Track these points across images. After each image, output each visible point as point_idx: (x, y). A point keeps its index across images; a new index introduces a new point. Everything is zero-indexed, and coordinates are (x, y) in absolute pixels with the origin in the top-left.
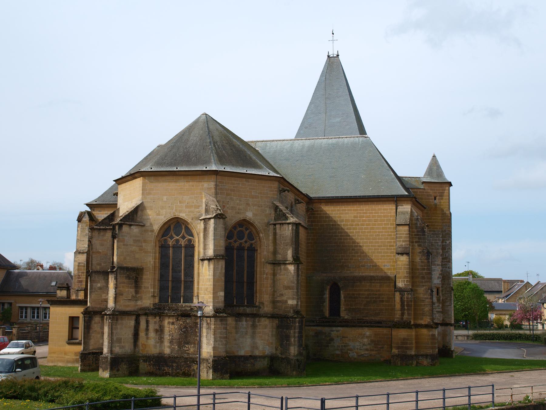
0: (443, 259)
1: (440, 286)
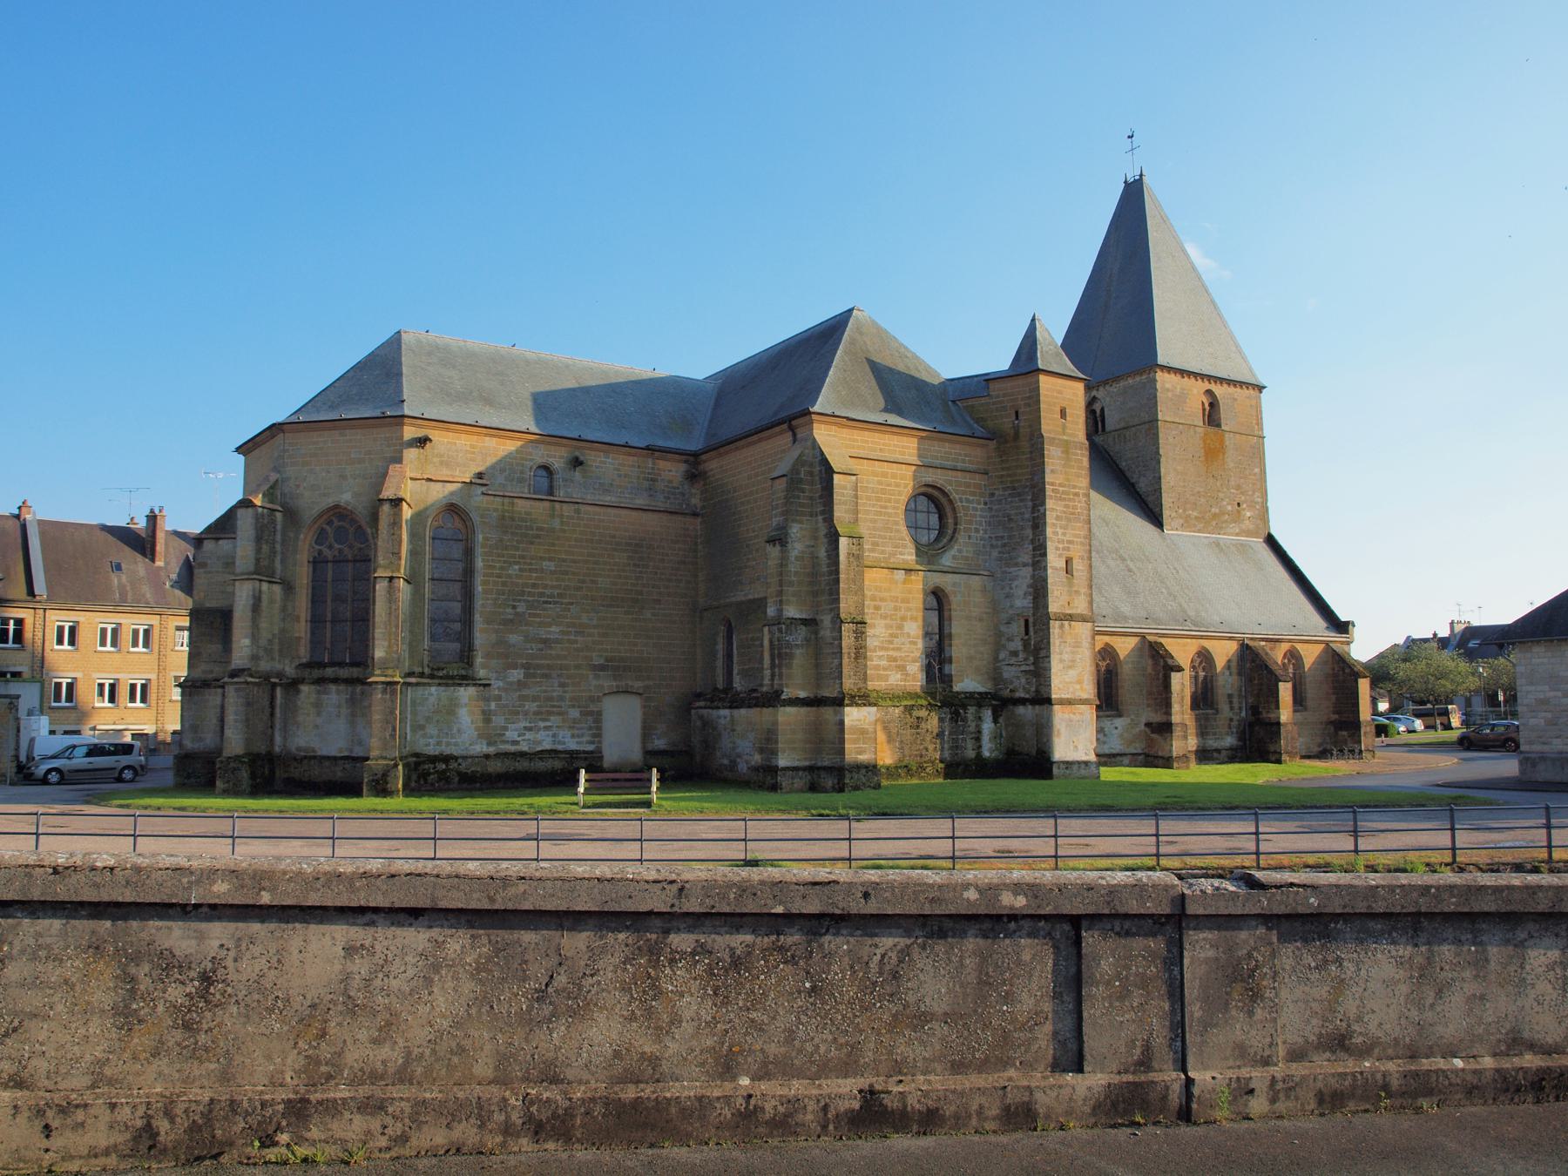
0: (1034, 549)
1: (1030, 613)
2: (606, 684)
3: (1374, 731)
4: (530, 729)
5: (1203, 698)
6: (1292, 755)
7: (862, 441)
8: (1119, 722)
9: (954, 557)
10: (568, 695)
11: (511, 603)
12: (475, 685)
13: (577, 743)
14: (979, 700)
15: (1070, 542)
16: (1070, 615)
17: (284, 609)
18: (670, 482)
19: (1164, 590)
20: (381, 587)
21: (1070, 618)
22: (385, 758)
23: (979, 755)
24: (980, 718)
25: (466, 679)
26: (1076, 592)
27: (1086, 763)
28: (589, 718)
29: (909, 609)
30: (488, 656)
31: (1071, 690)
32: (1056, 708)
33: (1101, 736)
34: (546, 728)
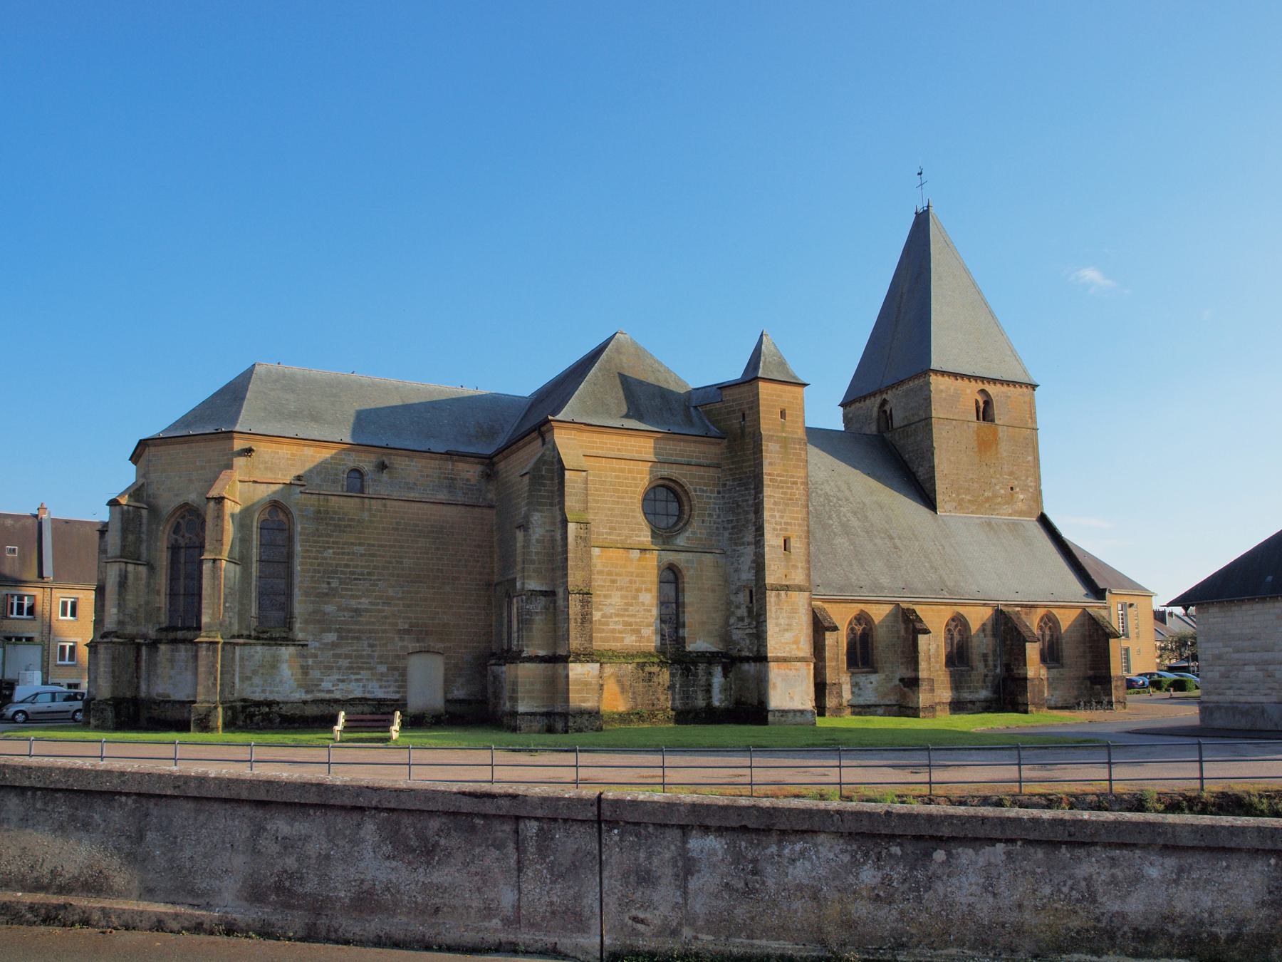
2: (410, 646)
3: (1125, 685)
4: (343, 681)
5: (958, 657)
6: (1039, 706)
7: (601, 443)
8: (873, 678)
9: (688, 538)
10: (376, 654)
11: (325, 580)
12: (294, 645)
13: (385, 692)
14: (709, 658)
15: (786, 523)
16: (787, 586)
17: (148, 585)
18: (468, 480)
19: (926, 564)
20: (207, 567)
21: (787, 588)
22: (209, 702)
23: (709, 705)
24: (710, 673)
25: (287, 640)
26: (793, 566)
27: (802, 712)
28: (395, 672)
29: (643, 582)
30: (306, 622)
31: (787, 649)
32: (772, 665)
33: (856, 690)
34: (357, 680)
